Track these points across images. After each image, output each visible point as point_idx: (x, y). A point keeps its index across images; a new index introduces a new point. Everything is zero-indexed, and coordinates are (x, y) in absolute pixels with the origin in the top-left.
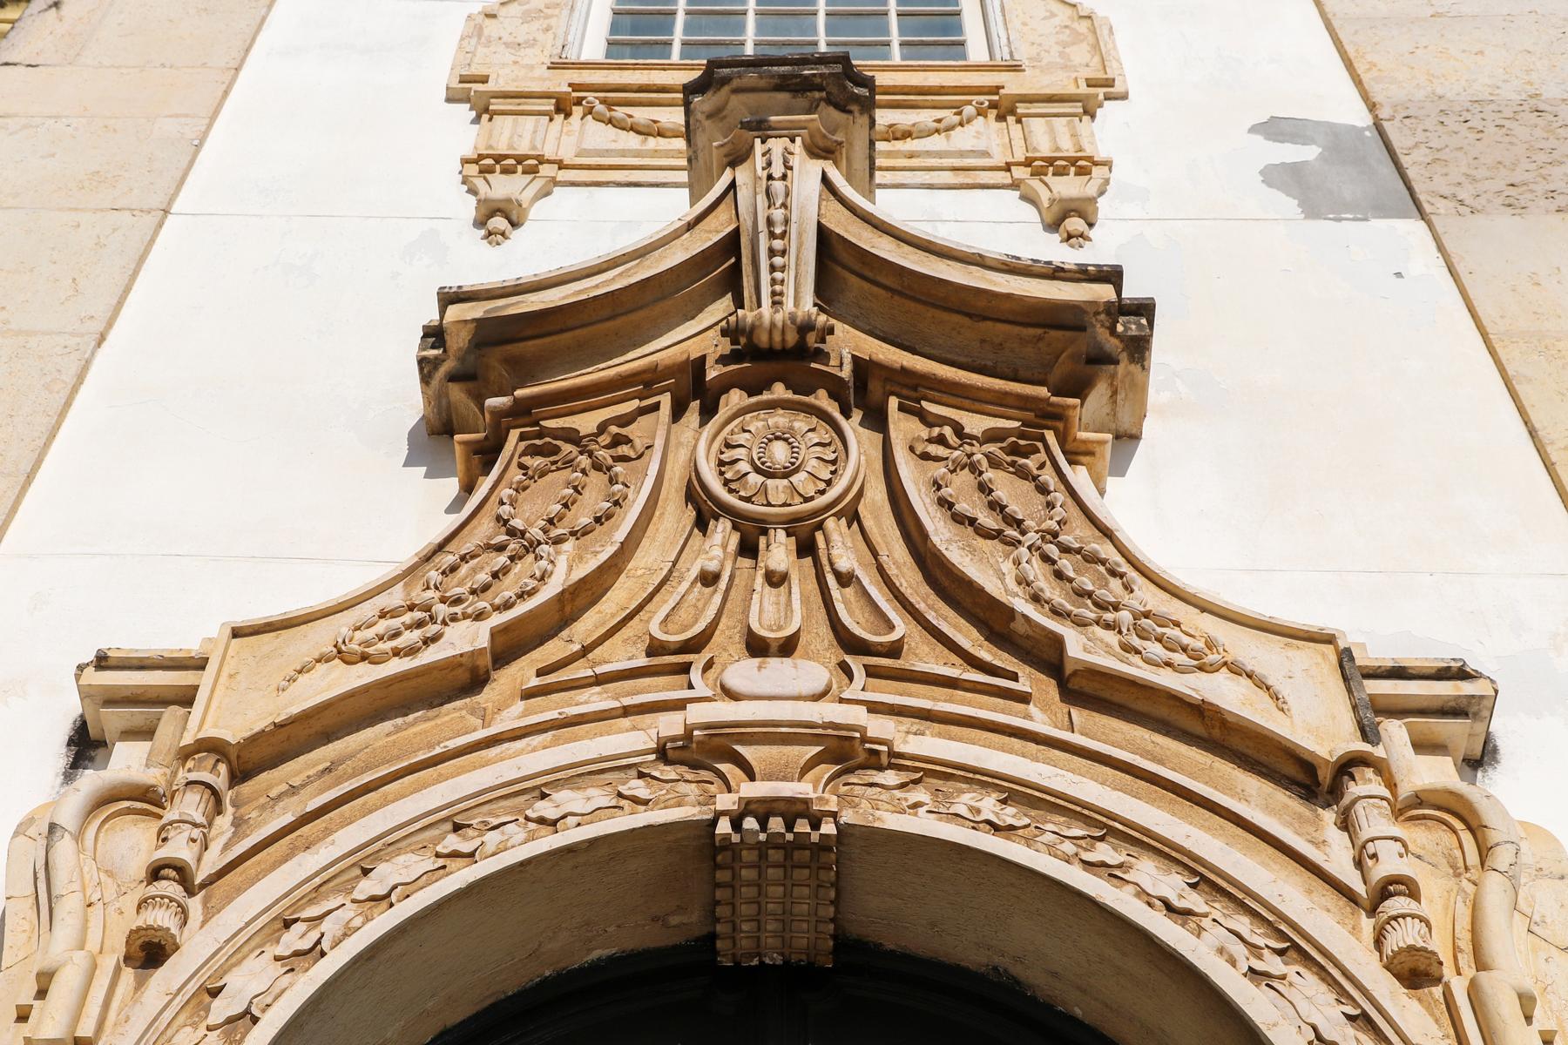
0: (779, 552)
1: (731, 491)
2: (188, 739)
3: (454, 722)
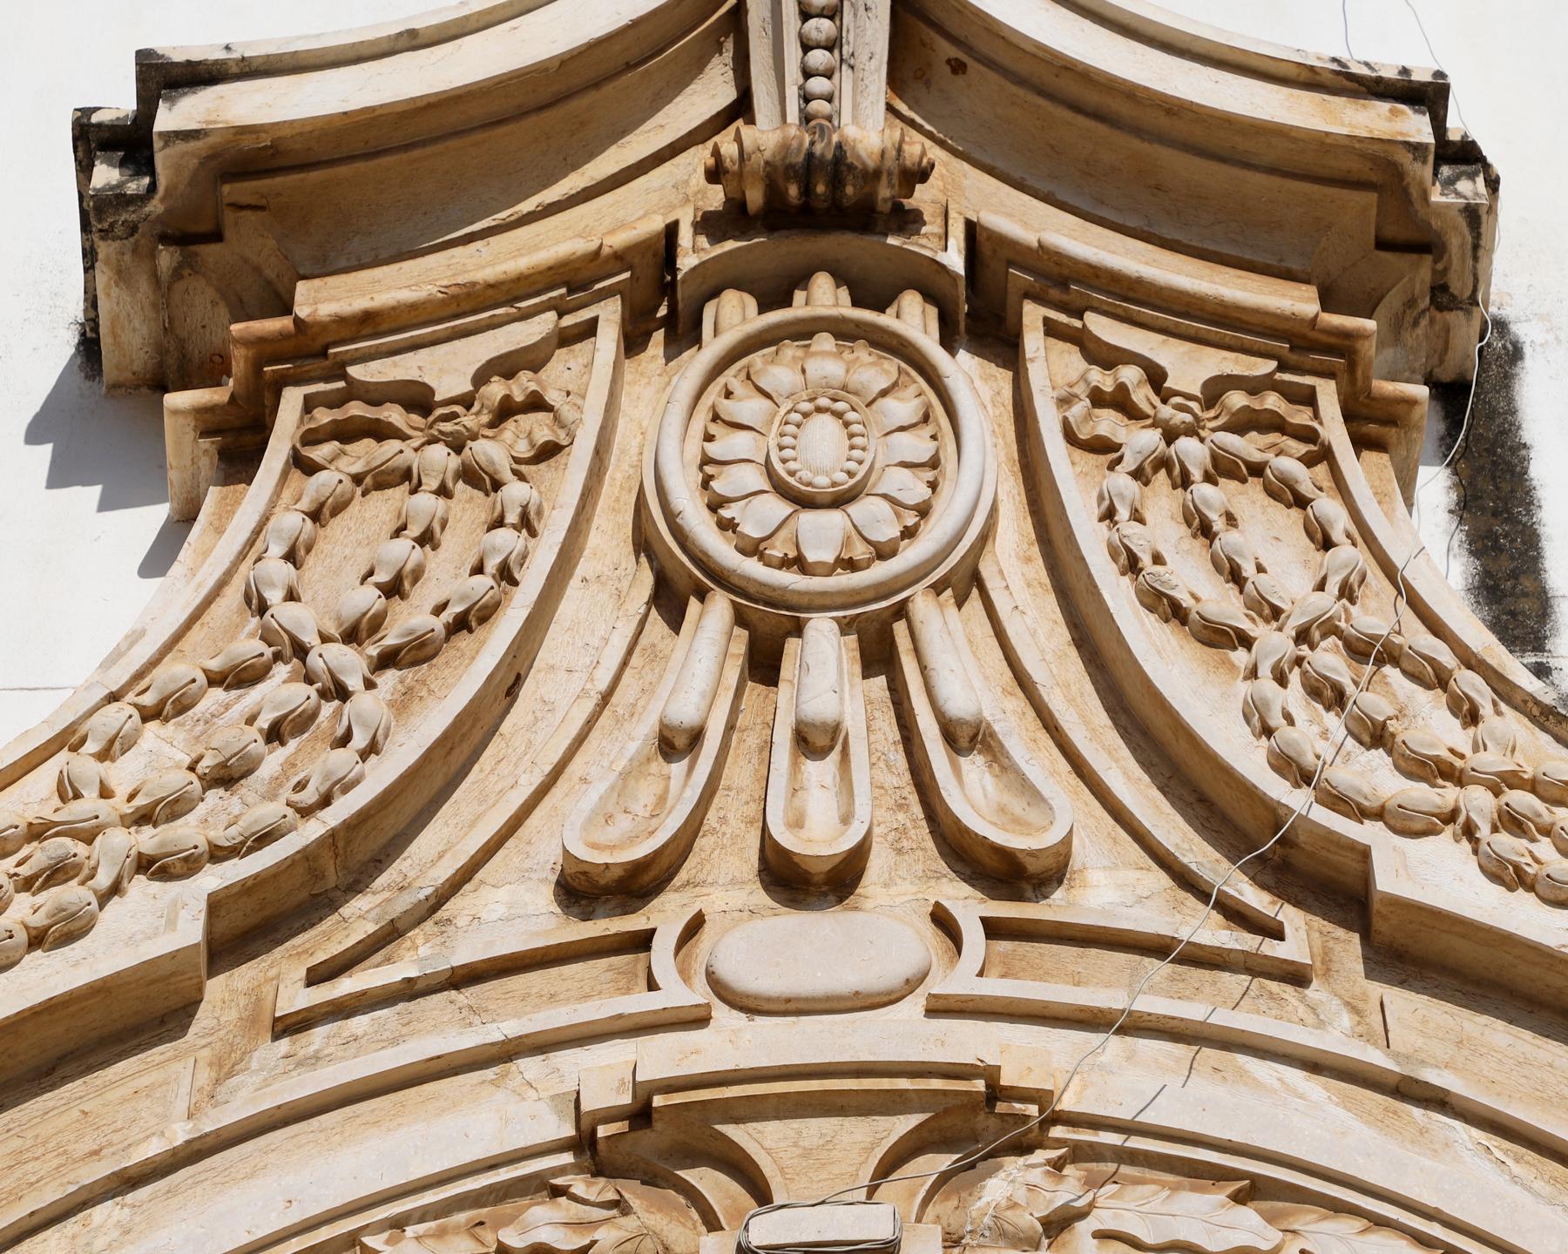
1: (727, 526)
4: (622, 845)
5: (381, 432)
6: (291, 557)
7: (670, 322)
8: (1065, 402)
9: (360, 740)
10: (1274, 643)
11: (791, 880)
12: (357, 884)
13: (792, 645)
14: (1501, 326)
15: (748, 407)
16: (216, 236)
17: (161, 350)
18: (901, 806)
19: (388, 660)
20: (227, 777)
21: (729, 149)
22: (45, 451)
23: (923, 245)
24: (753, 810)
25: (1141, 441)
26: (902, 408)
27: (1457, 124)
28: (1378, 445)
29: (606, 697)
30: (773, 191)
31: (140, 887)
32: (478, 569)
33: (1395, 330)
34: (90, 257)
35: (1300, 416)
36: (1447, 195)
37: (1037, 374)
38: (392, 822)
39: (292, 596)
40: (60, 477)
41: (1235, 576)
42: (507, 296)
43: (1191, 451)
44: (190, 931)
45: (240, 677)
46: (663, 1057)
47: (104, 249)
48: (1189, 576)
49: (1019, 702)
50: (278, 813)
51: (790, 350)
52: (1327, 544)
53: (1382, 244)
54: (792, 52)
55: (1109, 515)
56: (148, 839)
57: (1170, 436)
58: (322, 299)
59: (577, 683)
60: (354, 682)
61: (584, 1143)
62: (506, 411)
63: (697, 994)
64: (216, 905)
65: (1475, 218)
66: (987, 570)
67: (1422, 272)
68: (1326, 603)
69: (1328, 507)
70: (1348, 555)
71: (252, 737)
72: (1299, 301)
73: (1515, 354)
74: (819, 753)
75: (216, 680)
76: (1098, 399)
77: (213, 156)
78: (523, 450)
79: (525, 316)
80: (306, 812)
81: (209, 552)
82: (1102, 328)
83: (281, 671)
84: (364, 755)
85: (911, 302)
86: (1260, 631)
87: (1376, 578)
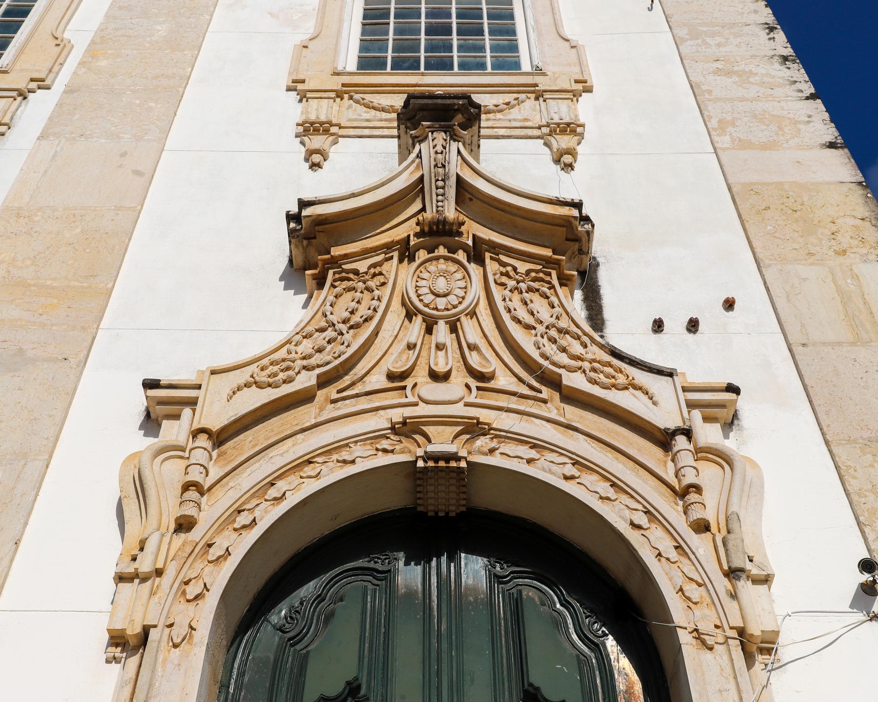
0: (442, 331)
1: (421, 300)
2: (196, 426)
3: (306, 415)
4: (400, 367)
5: (349, 279)
6: (331, 305)
7: (409, 256)
8: (494, 274)
9: (346, 344)
10: (541, 329)
11: (436, 377)
12: (346, 374)
13: (435, 326)
14: (594, 258)
15: (425, 275)
16: (315, 238)
17: (305, 262)
18: (459, 362)
19: (351, 327)
20: (320, 350)
21: (421, 218)
22: (283, 282)
23: (463, 239)
24: (427, 361)
25: (512, 283)
26: (459, 275)
27: (585, 212)
28: (566, 285)
29: (396, 336)
30: (430, 228)
31: (304, 372)
32: (369, 309)
33: (570, 259)
34: (290, 242)
35: (548, 278)
36: (582, 228)
37: (488, 268)
38: (353, 361)
39: (332, 314)
40: (286, 288)
41: (532, 314)
42: (374, 250)
43: (523, 286)
44: (314, 381)
45: (322, 330)
46: (408, 412)
47: (293, 241)
48: (522, 314)
49: (484, 340)
50: (330, 358)
51: (434, 262)
52: (553, 307)
53: (567, 240)
54: (434, 197)
55: (504, 300)
56: (305, 363)
57: (518, 282)
58: (336, 251)
59: (390, 333)
60: (344, 332)
61: (393, 428)
62: (374, 275)
63: (416, 399)
64: (318, 376)
65: (589, 234)
66: (477, 311)
67: (576, 246)
68: (553, 320)
69: (554, 299)
70: (558, 310)
71: (324, 343)
72: (548, 252)
73: (598, 265)
74: (441, 350)
75: (317, 331)
76: (502, 274)
77: (314, 221)
78: (378, 284)
79: (378, 255)
80: (335, 358)
81: (315, 304)
82: (503, 258)
83: (330, 329)
84: (347, 347)
85: (461, 252)
86: (538, 326)
87: (564, 315)
